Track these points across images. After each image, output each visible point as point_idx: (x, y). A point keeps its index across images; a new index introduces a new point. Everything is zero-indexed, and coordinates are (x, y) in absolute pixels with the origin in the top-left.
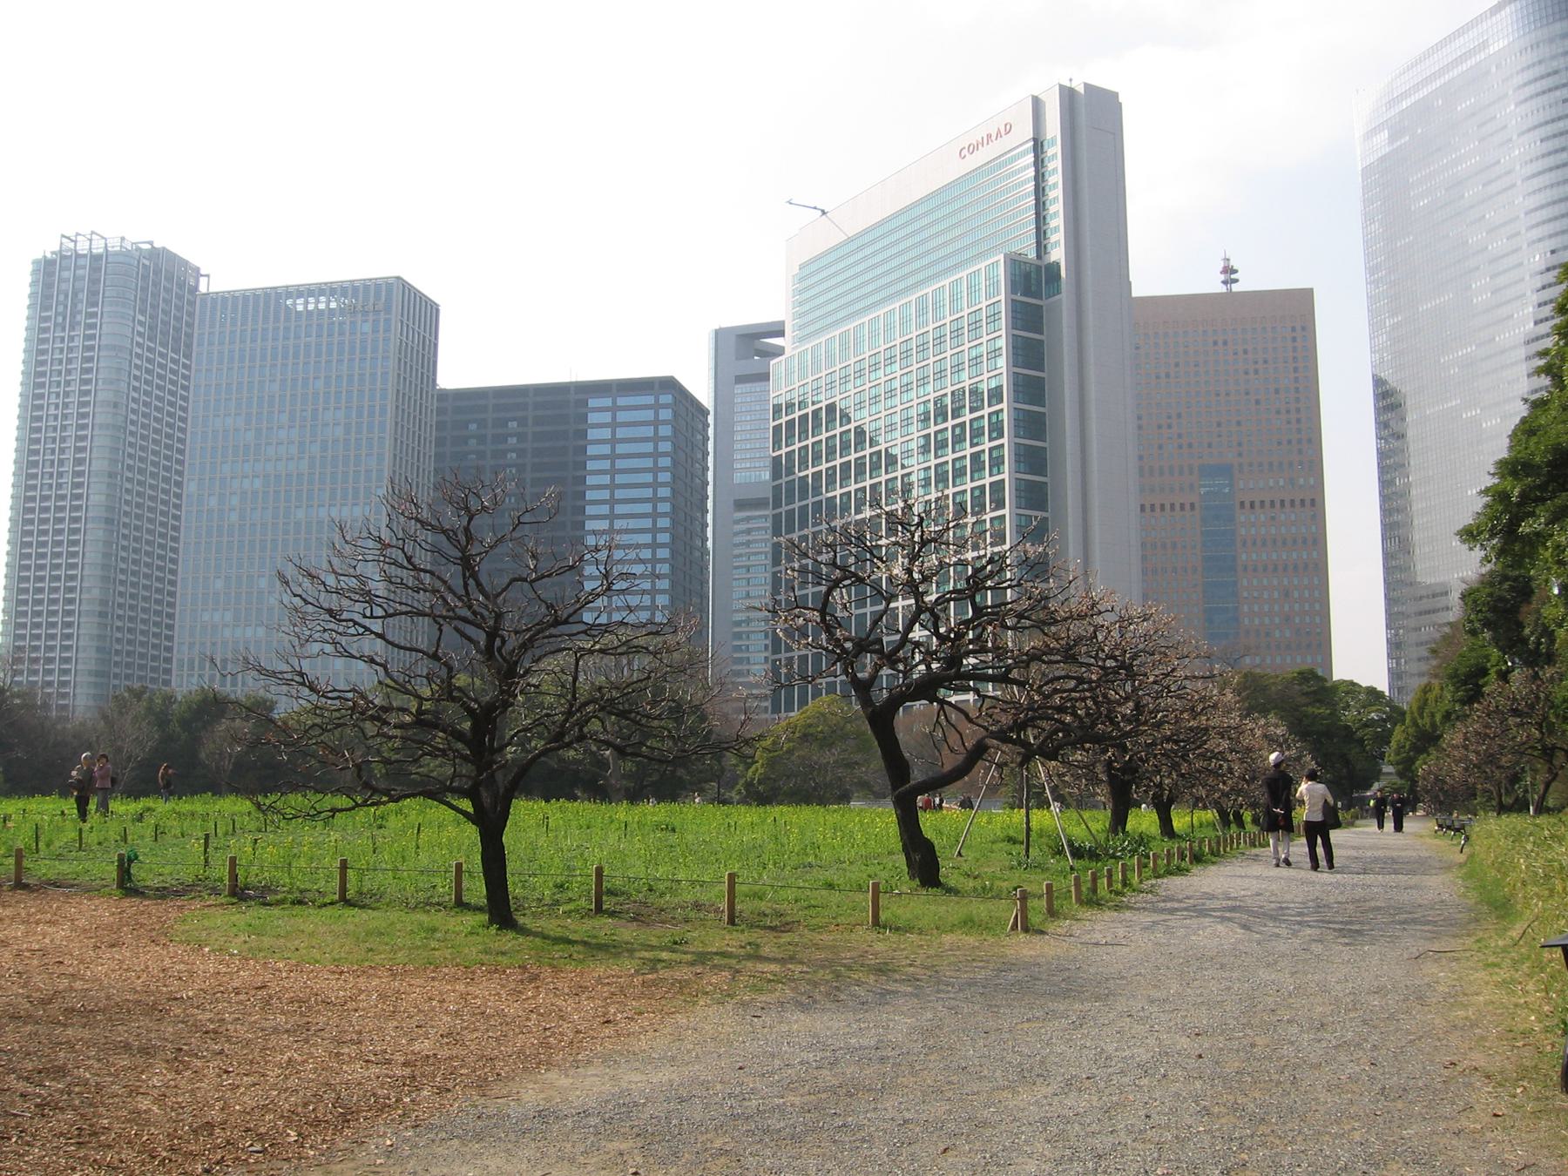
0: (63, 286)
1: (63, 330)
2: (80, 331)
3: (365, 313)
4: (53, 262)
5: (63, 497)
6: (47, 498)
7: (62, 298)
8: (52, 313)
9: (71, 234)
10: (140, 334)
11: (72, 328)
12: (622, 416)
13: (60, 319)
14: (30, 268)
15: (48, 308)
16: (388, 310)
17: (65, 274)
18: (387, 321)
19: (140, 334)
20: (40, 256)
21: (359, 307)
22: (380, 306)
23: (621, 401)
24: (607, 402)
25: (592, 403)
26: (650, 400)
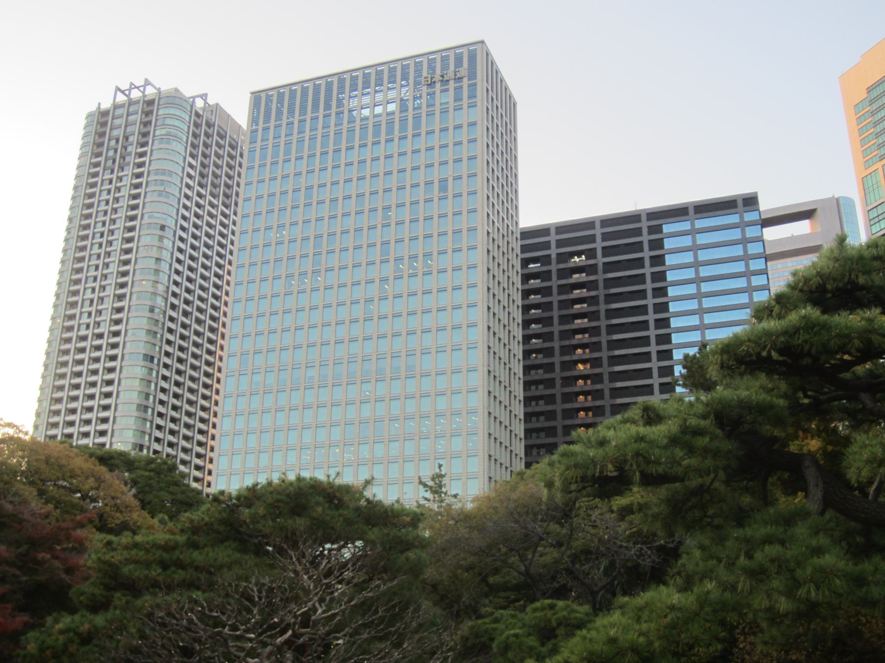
0: (115, 133)
1: (112, 172)
2: (129, 171)
3: (444, 82)
4: (105, 114)
5: (100, 336)
6: (84, 338)
7: (113, 143)
8: (102, 159)
9: (125, 86)
10: (190, 176)
11: (122, 168)
12: (702, 239)
13: (110, 163)
14: (83, 122)
15: (99, 155)
16: (472, 75)
17: (117, 122)
18: (472, 87)
19: (190, 176)
20: (93, 108)
21: (437, 77)
22: (464, 71)
23: (700, 224)
24: (685, 226)
25: (667, 229)
26: (734, 219)
